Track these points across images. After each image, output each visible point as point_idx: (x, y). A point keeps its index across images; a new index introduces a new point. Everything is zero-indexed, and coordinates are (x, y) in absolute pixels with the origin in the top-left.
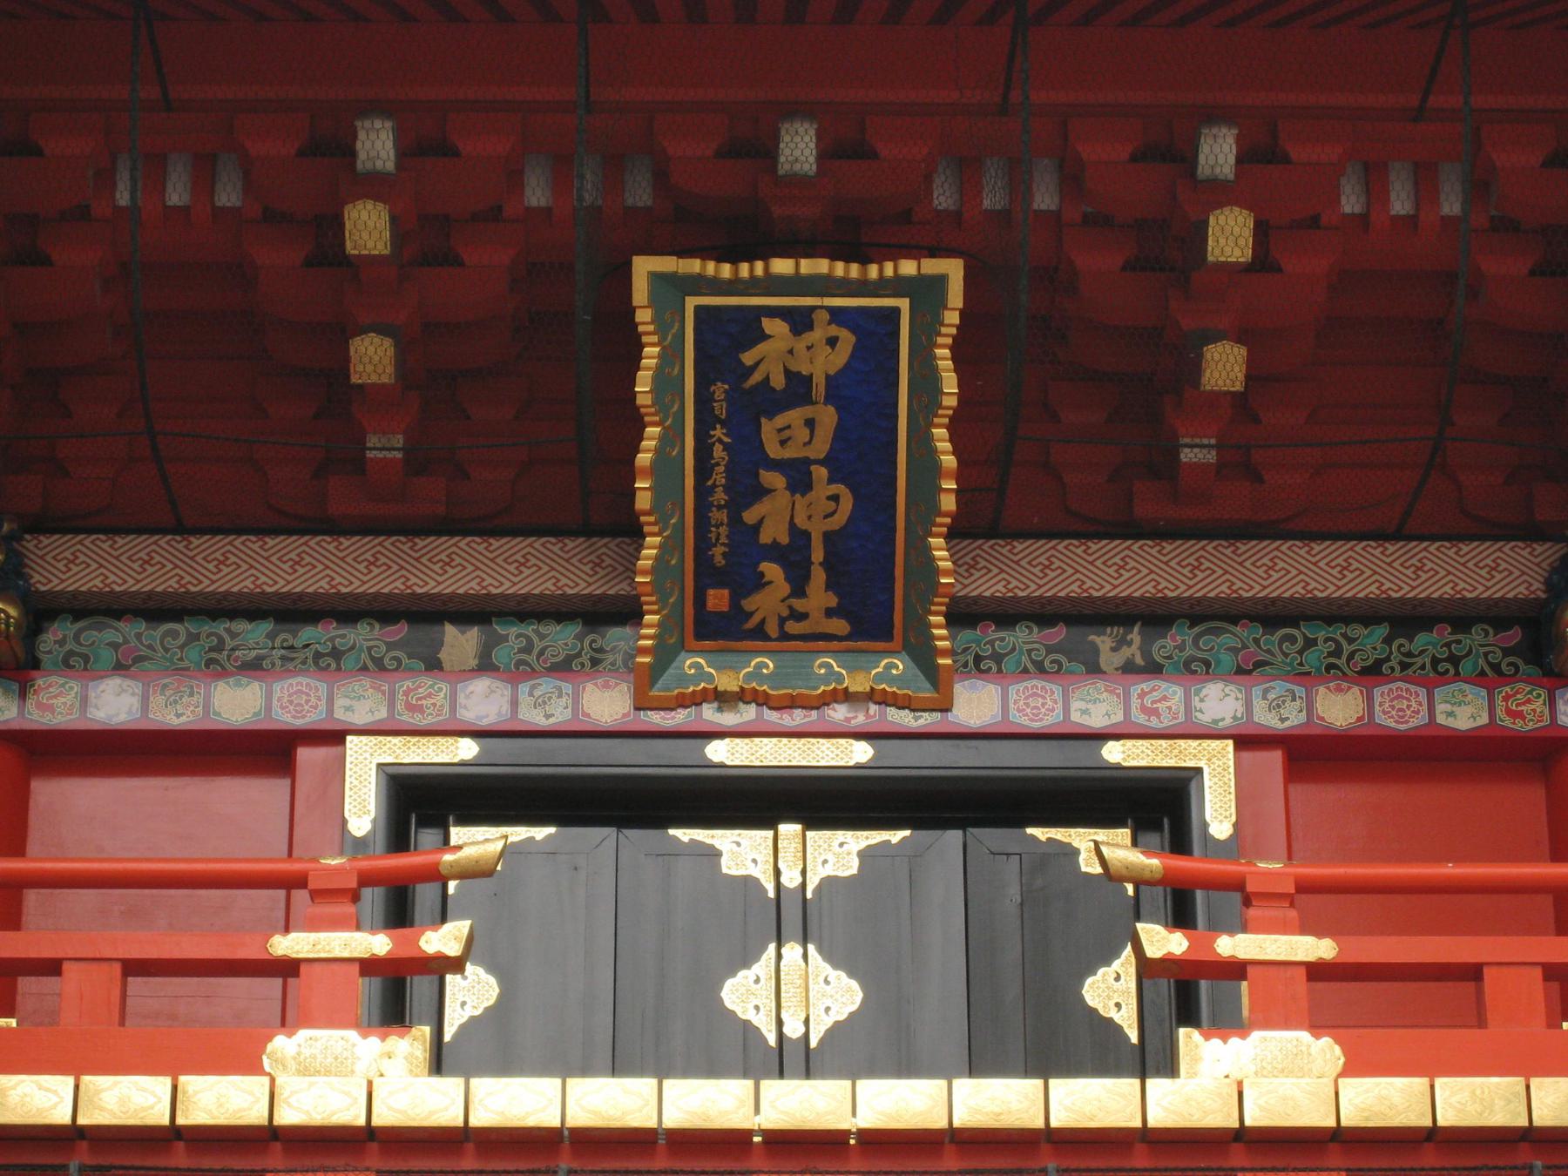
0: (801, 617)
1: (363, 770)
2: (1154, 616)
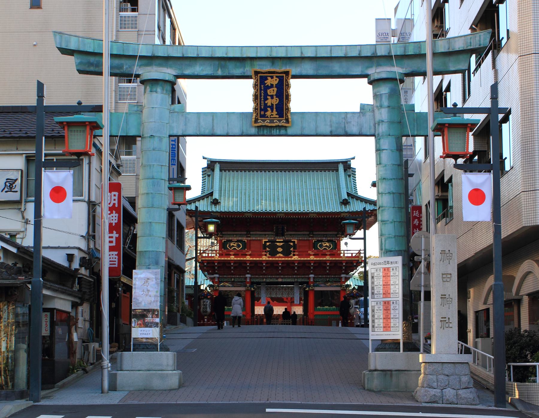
0: (272, 115)
1: (264, 240)
2: (294, 234)
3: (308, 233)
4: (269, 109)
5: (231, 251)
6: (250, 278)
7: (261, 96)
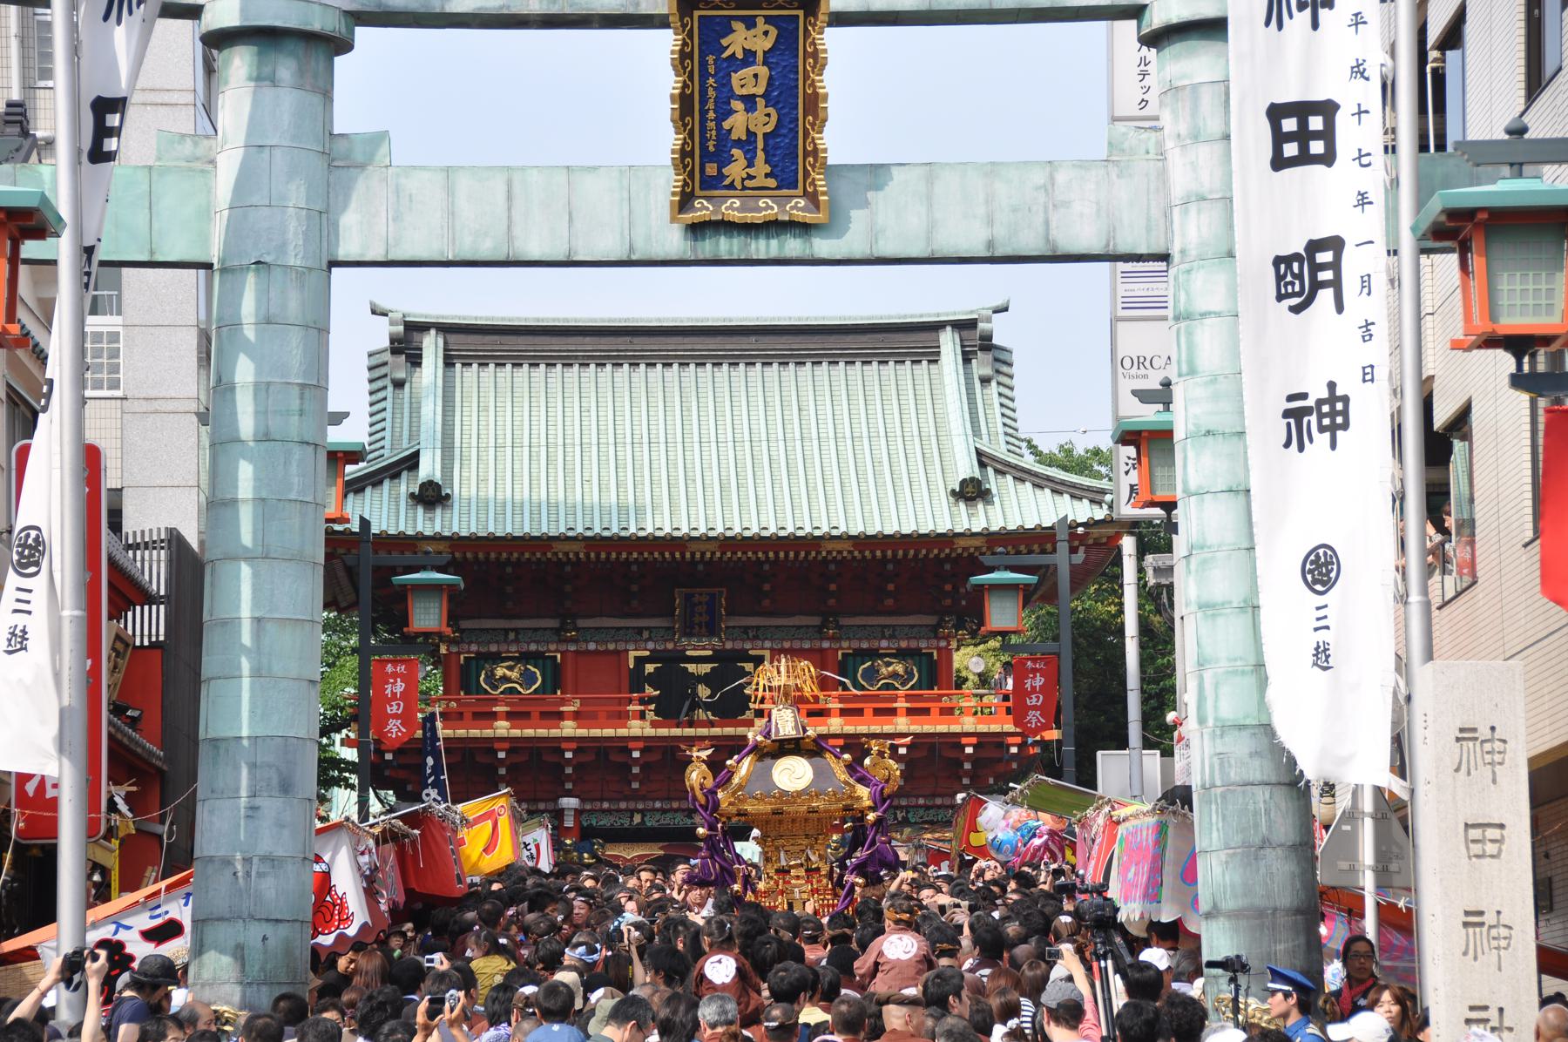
3: (816, 621)
4: (736, 152)
5: (495, 701)
6: (578, 813)
7: (703, 101)
